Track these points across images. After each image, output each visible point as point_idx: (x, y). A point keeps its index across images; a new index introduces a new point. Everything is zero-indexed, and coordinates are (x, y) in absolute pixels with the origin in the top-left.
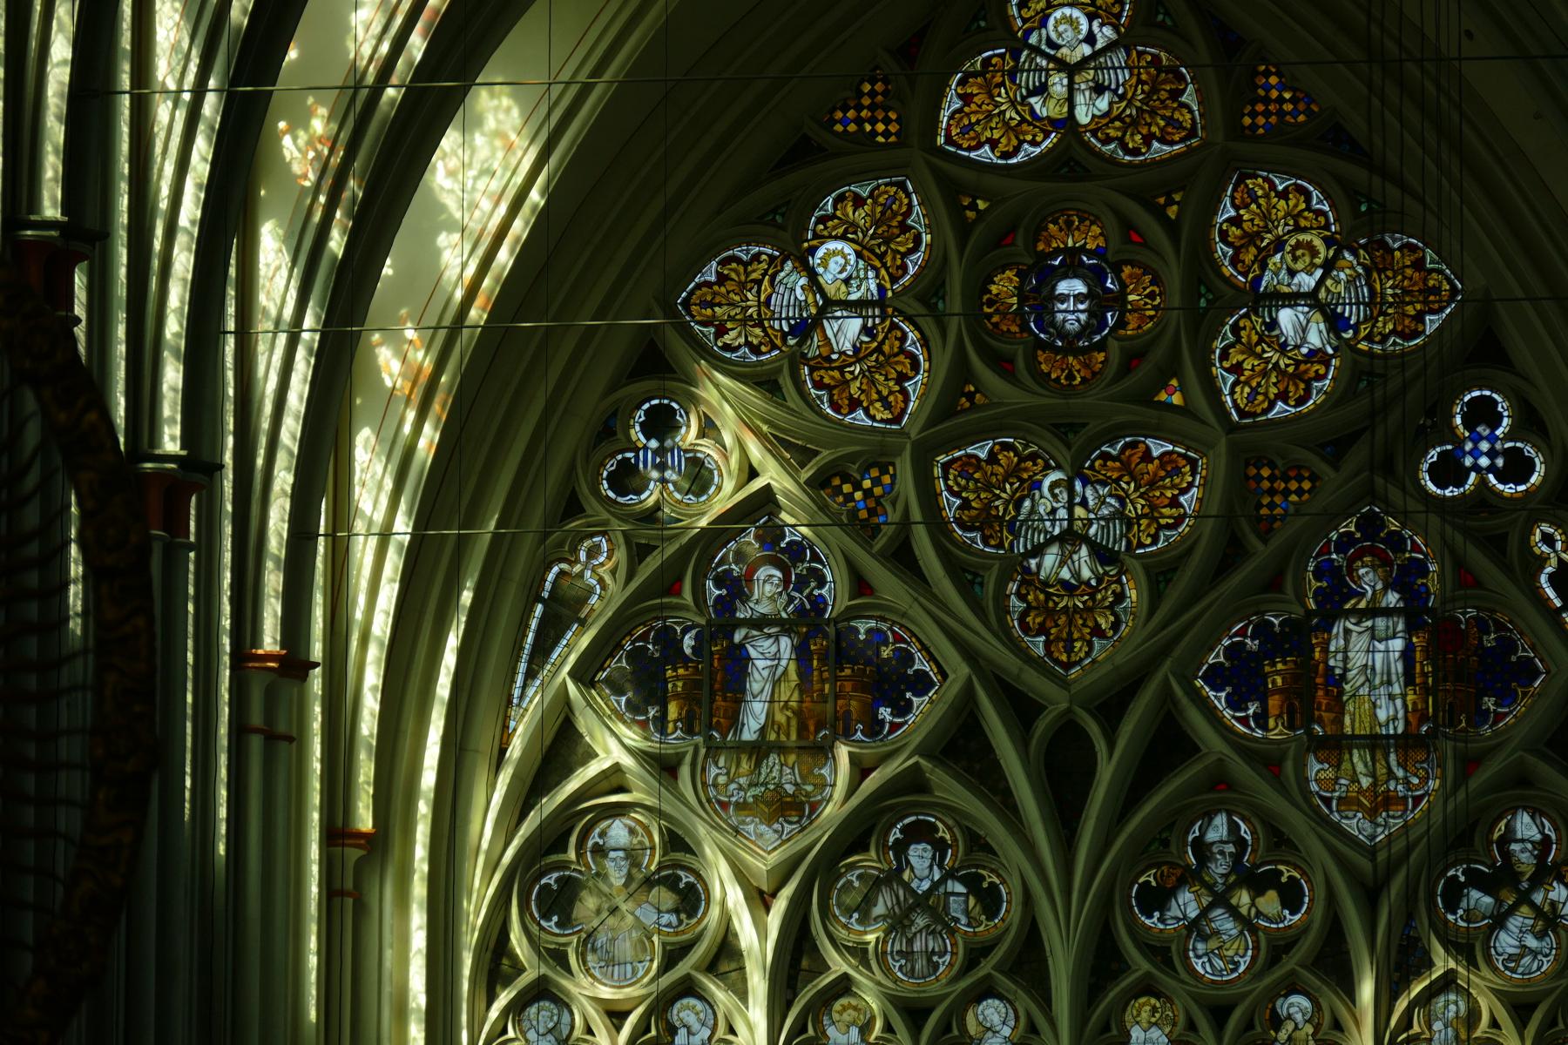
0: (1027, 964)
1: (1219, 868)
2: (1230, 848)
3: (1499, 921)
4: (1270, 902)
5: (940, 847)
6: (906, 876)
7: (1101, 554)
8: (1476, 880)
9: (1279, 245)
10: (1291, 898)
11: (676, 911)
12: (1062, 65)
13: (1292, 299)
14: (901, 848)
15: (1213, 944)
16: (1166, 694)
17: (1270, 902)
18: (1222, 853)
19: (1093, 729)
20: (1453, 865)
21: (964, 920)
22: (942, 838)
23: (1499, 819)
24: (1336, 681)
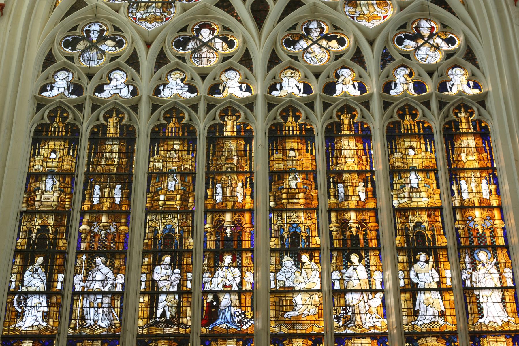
0: (246, 59)
1: (315, 35)
2: (319, 30)
3: (417, 48)
4: (334, 44)
5: (213, 30)
6: (200, 37)
8: (408, 37)
10: (341, 42)
11: (115, 47)
14: (198, 31)
15: (313, 54)
17: (334, 44)
18: (315, 31)
20: (399, 33)
21: (221, 49)
22: (213, 28)
23: (415, 21)
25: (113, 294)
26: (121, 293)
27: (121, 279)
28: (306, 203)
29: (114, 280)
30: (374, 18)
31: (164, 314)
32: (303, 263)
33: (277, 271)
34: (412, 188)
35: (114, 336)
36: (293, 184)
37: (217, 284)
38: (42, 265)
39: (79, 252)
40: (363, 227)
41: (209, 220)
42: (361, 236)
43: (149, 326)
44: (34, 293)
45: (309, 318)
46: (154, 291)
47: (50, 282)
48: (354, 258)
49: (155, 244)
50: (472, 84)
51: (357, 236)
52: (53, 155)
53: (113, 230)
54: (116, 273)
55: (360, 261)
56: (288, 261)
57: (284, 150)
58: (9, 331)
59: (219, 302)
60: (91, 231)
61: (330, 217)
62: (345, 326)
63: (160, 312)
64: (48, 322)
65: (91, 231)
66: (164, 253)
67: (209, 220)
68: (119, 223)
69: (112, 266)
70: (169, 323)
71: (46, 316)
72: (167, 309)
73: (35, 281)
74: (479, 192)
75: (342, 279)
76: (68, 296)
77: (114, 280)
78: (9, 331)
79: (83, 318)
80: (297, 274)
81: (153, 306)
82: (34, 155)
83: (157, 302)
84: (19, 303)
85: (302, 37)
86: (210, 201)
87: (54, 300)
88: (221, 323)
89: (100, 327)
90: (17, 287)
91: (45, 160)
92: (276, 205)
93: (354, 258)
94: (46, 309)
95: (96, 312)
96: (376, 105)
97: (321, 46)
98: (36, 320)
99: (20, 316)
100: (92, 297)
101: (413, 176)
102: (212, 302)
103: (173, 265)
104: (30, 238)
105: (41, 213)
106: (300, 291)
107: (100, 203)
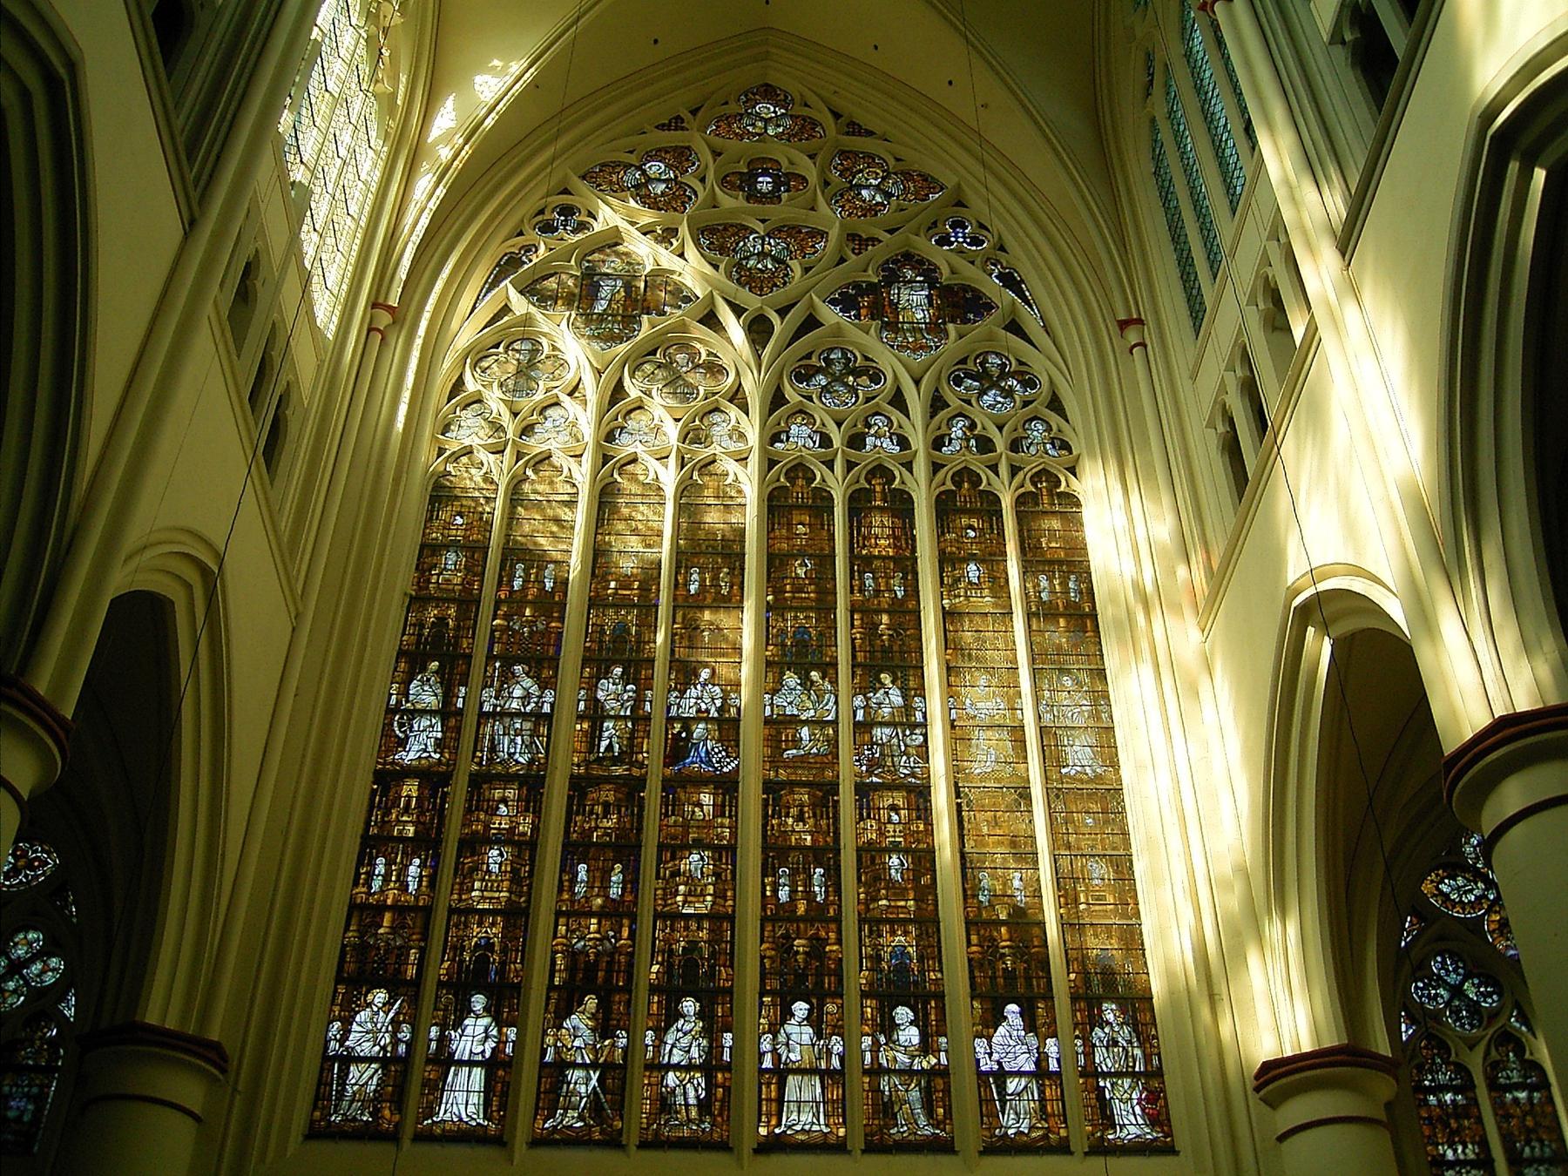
7: (775, 259)
8: (969, 375)
9: (861, 171)
12: (762, 119)
13: (867, 187)
16: (812, 305)
19: (775, 318)
24: (894, 306)
25: (538, 717)
26: (549, 717)
27: (549, 696)
28: (817, 600)
29: (540, 697)
30: (921, 348)
31: (610, 747)
32: (812, 683)
33: (774, 692)
34: (970, 583)
35: (538, 776)
36: (801, 572)
37: (688, 707)
38: (436, 672)
39: (491, 658)
40: (899, 634)
41: (679, 618)
42: (895, 648)
43: (588, 763)
44: (424, 712)
45: (819, 759)
46: (596, 715)
47: (448, 696)
48: (886, 678)
49: (600, 649)
50: (1057, 443)
51: (891, 646)
52: (459, 520)
53: (541, 627)
54: (542, 688)
55: (893, 682)
56: (791, 679)
57: (790, 524)
58: (385, 764)
59: (690, 734)
60: (508, 628)
61: (852, 619)
62: (870, 773)
63: (604, 744)
64: (441, 753)
65: (508, 628)
66: (616, 663)
67: (679, 618)
68: (550, 618)
69: (537, 678)
70: (616, 761)
71: (440, 745)
72: (615, 739)
73: (426, 695)
74: (1066, 591)
75: (866, 707)
76: (471, 720)
77: (540, 697)
78: (385, 764)
79: (493, 749)
80: (804, 698)
81: (594, 735)
82: (431, 519)
83: (601, 731)
84: (401, 725)
85: (819, 370)
86: (681, 592)
87: (452, 722)
88: (693, 764)
89: (517, 762)
90: (399, 702)
91: (448, 525)
92: (776, 600)
93: (886, 678)
94: (439, 735)
95: (512, 741)
96: (921, 466)
97: (846, 385)
98: (425, 751)
99: (402, 743)
100: (507, 720)
101: (972, 567)
102: (680, 733)
103: (626, 678)
104: (420, 635)
105: (438, 601)
106: (806, 722)
107: (524, 588)
